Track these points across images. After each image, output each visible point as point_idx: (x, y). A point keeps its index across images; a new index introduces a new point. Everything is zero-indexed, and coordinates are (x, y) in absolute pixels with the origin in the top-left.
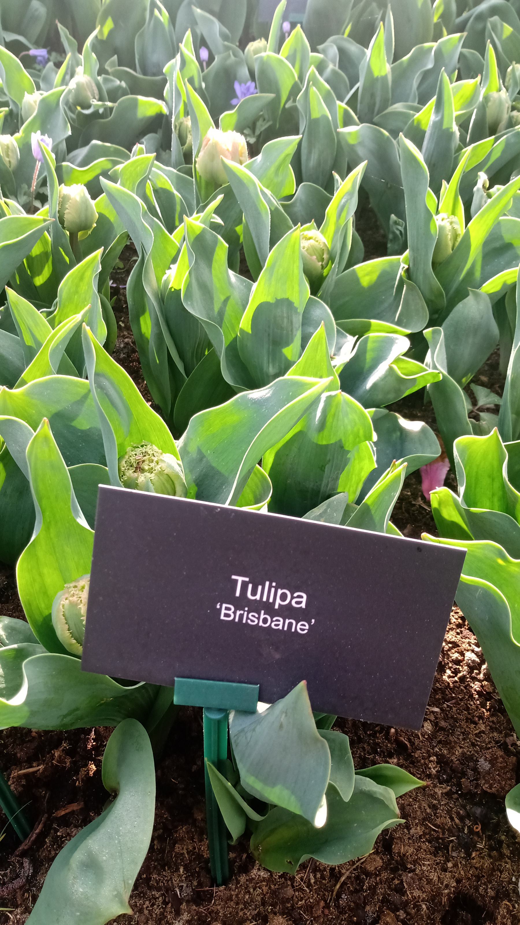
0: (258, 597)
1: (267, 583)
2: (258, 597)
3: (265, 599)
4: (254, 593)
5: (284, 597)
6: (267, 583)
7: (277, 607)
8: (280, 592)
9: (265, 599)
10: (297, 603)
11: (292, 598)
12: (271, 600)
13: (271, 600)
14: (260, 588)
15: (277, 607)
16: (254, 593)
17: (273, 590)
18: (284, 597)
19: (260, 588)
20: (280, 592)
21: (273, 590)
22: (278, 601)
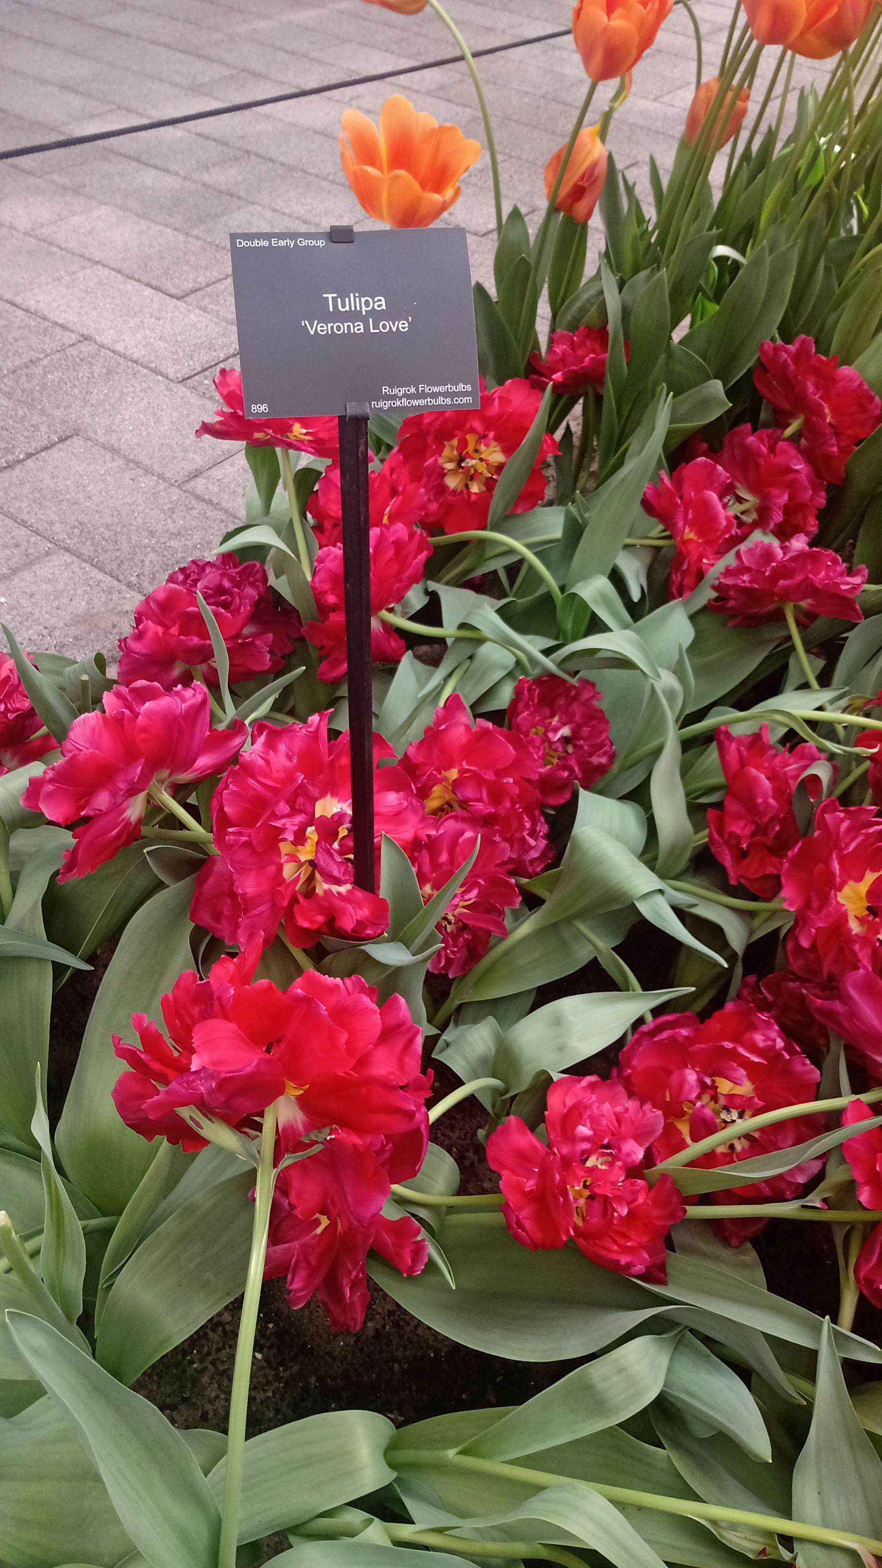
0: (347, 308)
1: (352, 295)
2: (347, 308)
3: (353, 309)
4: (344, 306)
5: (367, 304)
6: (352, 295)
7: (364, 313)
9: (353, 309)
10: (379, 306)
11: (374, 303)
12: (358, 309)
13: (358, 309)
14: (347, 300)
15: (364, 313)
16: (344, 306)
17: (357, 299)
18: (367, 304)
19: (347, 300)
20: (363, 300)
21: (357, 299)
22: (364, 308)
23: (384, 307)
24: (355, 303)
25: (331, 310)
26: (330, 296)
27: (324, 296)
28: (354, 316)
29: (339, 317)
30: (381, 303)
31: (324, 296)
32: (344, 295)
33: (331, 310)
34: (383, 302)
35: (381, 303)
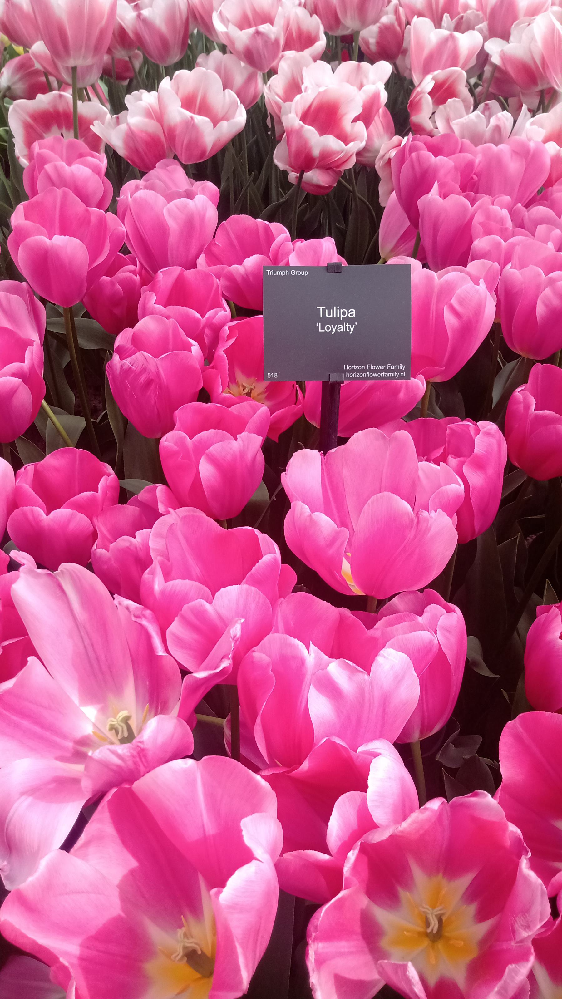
0: (331, 316)
1: (335, 308)
2: (331, 316)
4: (329, 314)
5: (344, 313)
6: (335, 308)
8: (342, 311)
10: (351, 315)
11: (348, 313)
12: (338, 316)
13: (338, 316)
14: (332, 310)
16: (329, 314)
18: (344, 313)
19: (332, 310)
20: (342, 311)
22: (342, 316)
23: (354, 316)
24: (336, 312)
25: (321, 316)
26: (321, 308)
27: (318, 307)
28: (336, 321)
29: (325, 321)
30: (352, 313)
31: (318, 307)
32: (329, 308)
33: (321, 316)
34: (354, 313)
35: (352, 313)
